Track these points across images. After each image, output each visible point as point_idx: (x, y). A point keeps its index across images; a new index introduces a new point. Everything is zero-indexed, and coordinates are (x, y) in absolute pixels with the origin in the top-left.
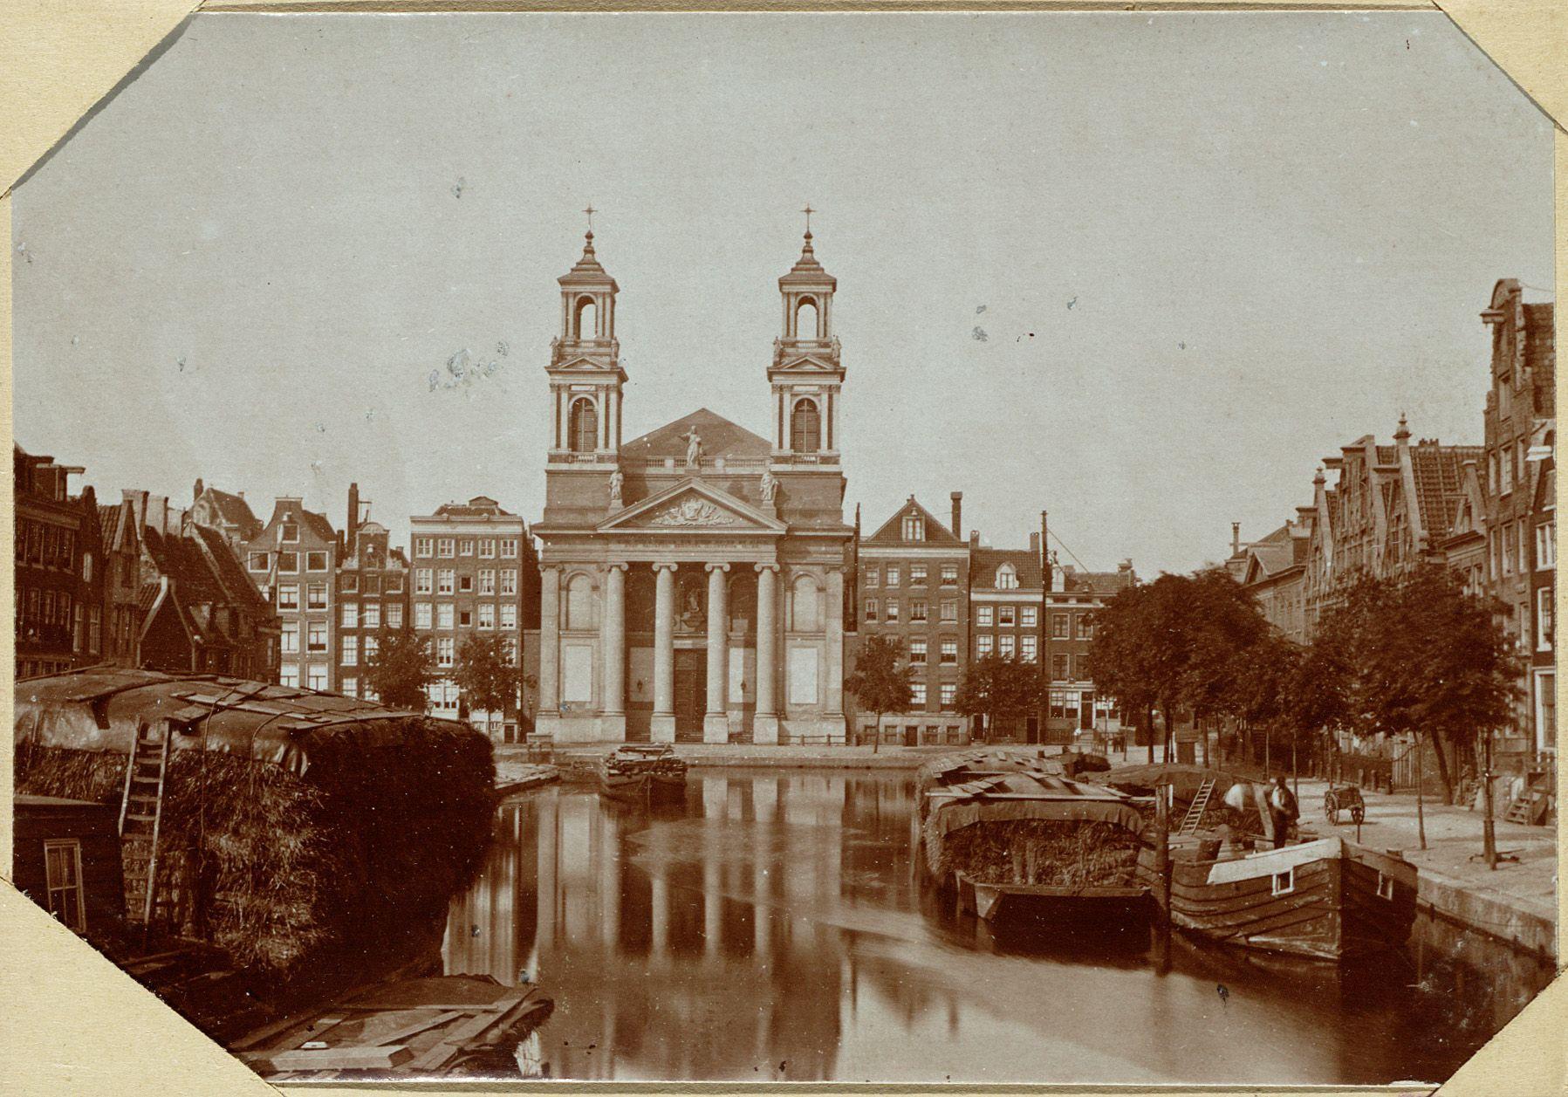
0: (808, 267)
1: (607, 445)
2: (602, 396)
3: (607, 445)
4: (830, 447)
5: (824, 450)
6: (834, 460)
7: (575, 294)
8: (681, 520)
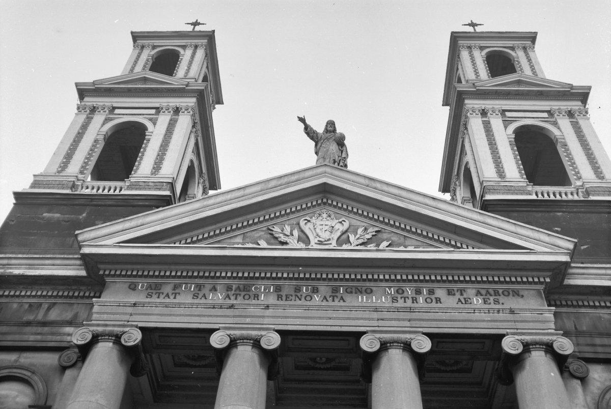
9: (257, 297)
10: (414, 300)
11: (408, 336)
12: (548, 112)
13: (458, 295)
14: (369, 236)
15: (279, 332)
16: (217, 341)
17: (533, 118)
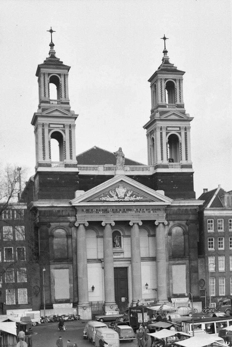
0: (167, 67)
1: (71, 158)
2: (67, 130)
3: (71, 158)
4: (187, 159)
5: (184, 162)
6: (190, 166)
7: (49, 74)
8: (116, 198)
9: (109, 212)
10: (140, 212)
11: (137, 222)
12: (180, 127)
13: (148, 211)
14: (131, 194)
15: (114, 221)
16: (103, 224)
17: (175, 130)
